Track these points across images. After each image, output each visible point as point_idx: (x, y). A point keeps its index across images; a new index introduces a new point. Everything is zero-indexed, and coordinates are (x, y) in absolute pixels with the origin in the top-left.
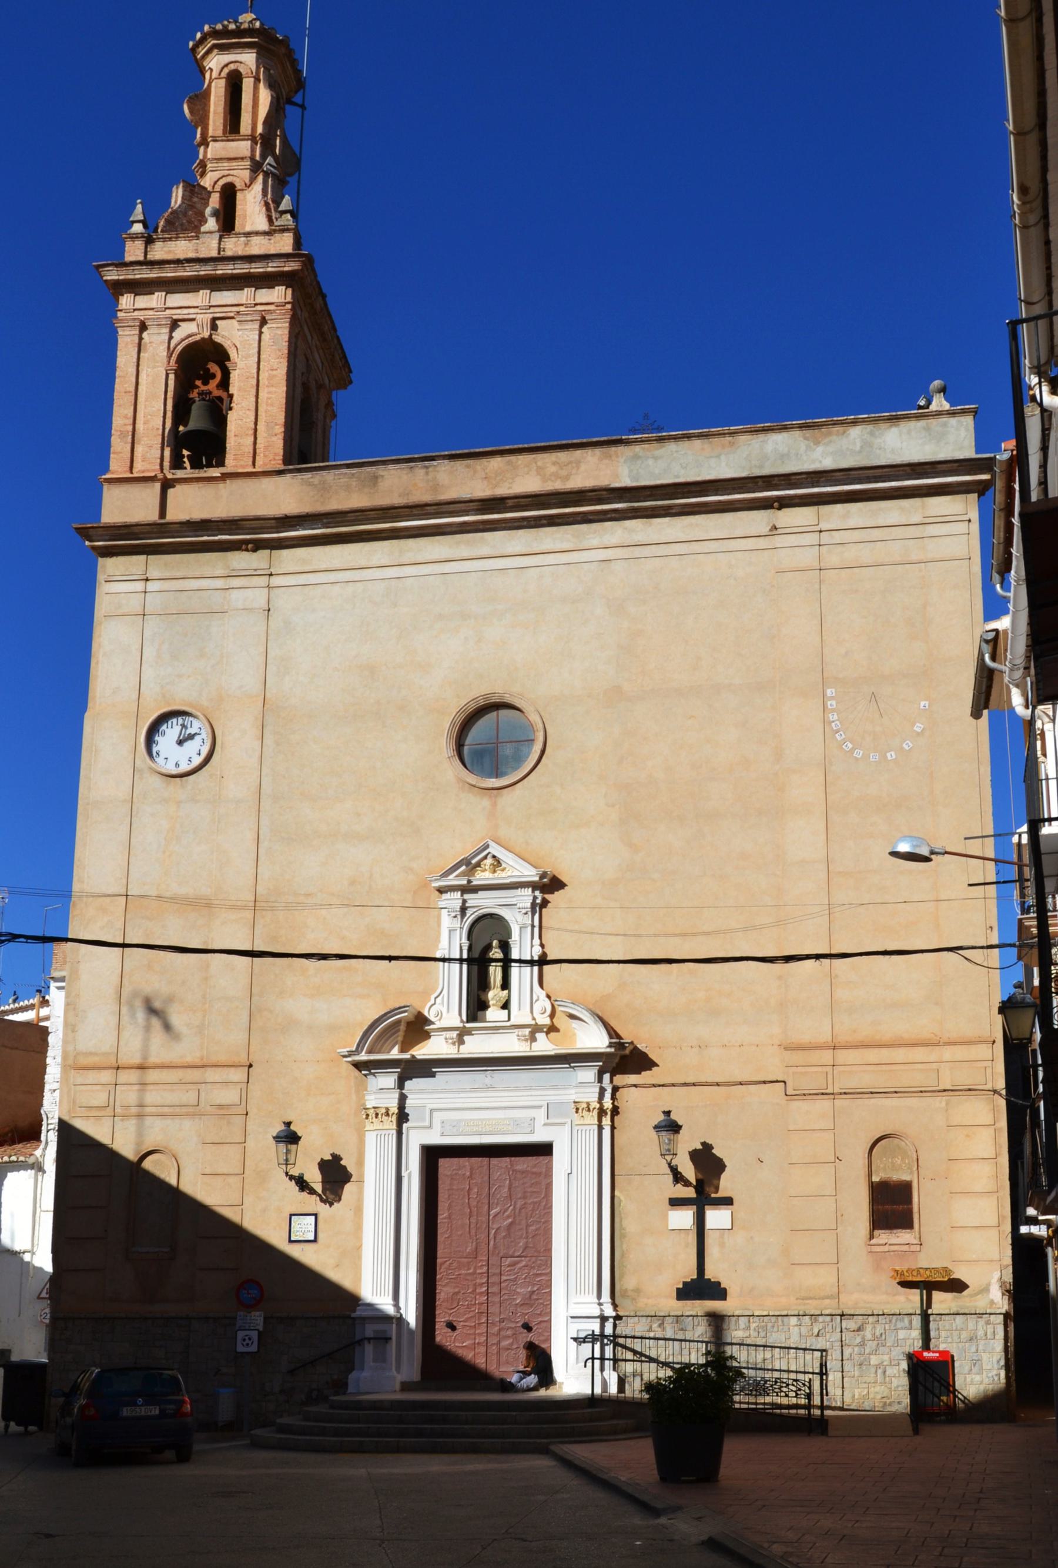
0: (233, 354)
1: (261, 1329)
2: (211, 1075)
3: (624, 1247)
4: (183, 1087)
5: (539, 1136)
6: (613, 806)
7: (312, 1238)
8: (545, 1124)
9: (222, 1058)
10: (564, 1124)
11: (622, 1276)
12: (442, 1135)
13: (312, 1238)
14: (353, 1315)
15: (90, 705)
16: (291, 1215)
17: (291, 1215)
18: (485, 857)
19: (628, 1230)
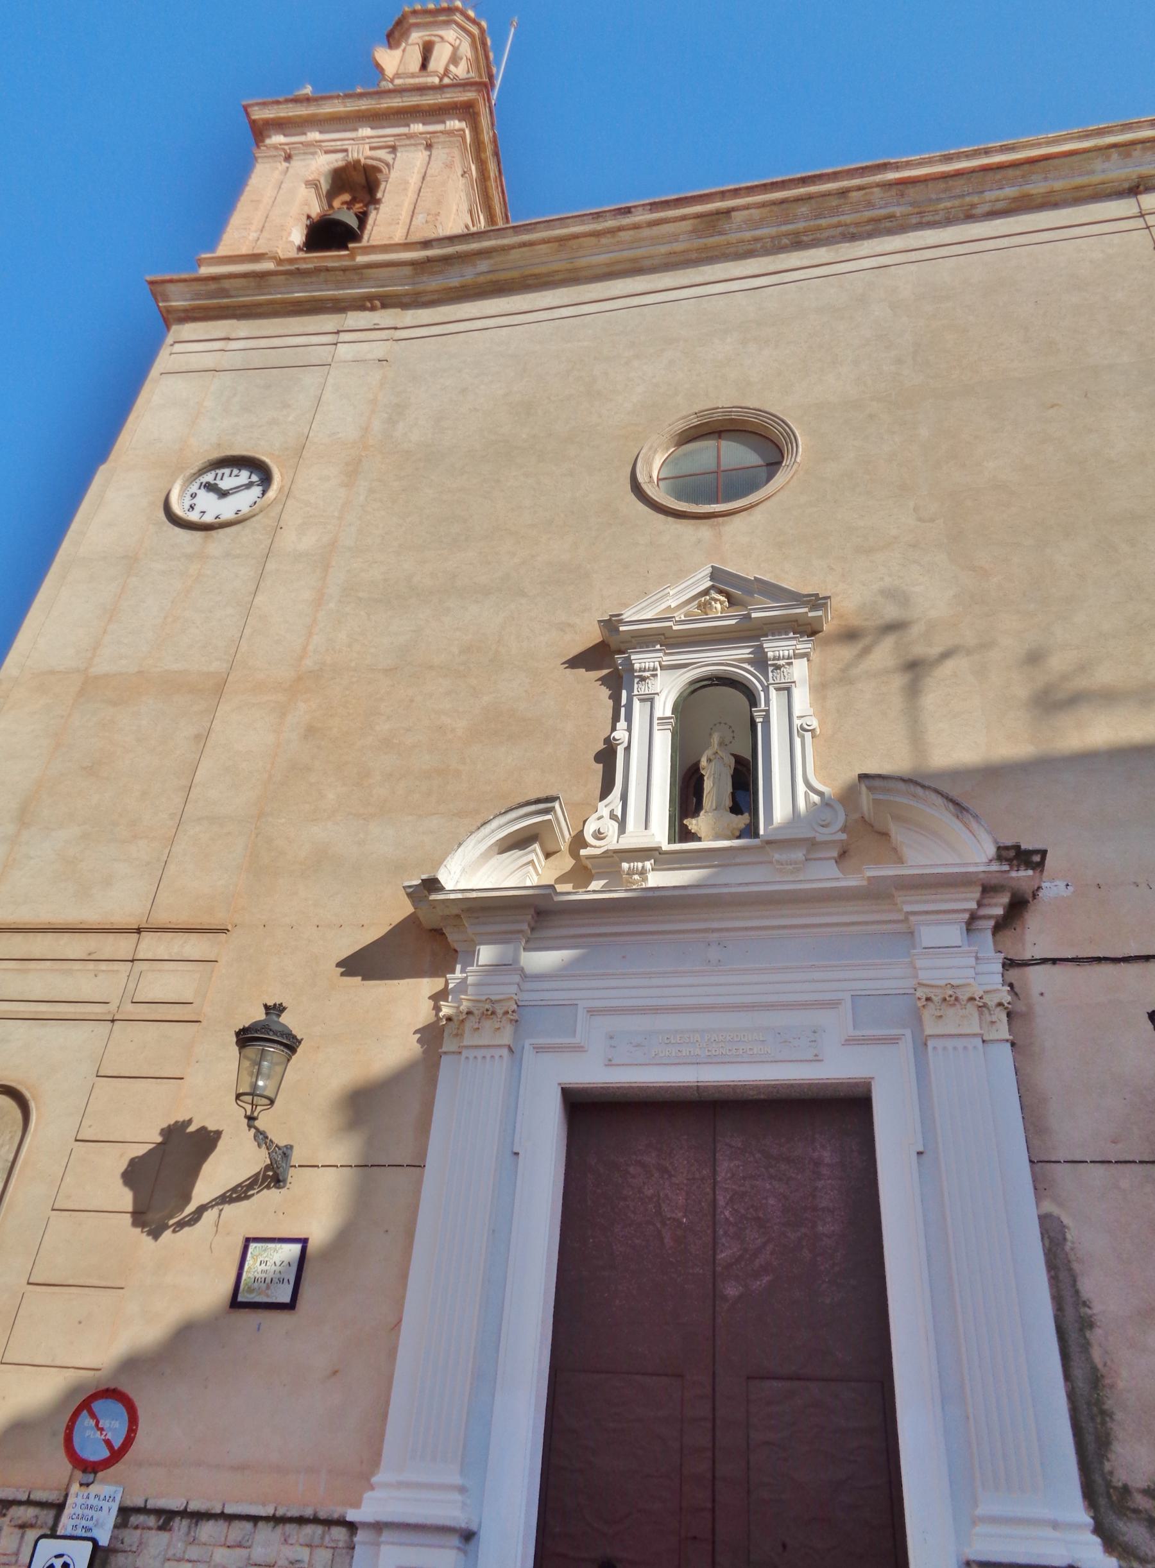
0: (385, 170)
1: (104, 1541)
2: (150, 945)
3: (1096, 1354)
4: (91, 965)
5: (833, 1067)
6: (932, 520)
7: (286, 1299)
8: (850, 1041)
9: (182, 918)
10: (893, 1040)
11: (1104, 1442)
12: (610, 1063)
13: (286, 1299)
14: (352, 1515)
15: (112, 457)
16: (248, 1241)
17: (248, 1241)
18: (706, 592)
19: (1097, 1308)
